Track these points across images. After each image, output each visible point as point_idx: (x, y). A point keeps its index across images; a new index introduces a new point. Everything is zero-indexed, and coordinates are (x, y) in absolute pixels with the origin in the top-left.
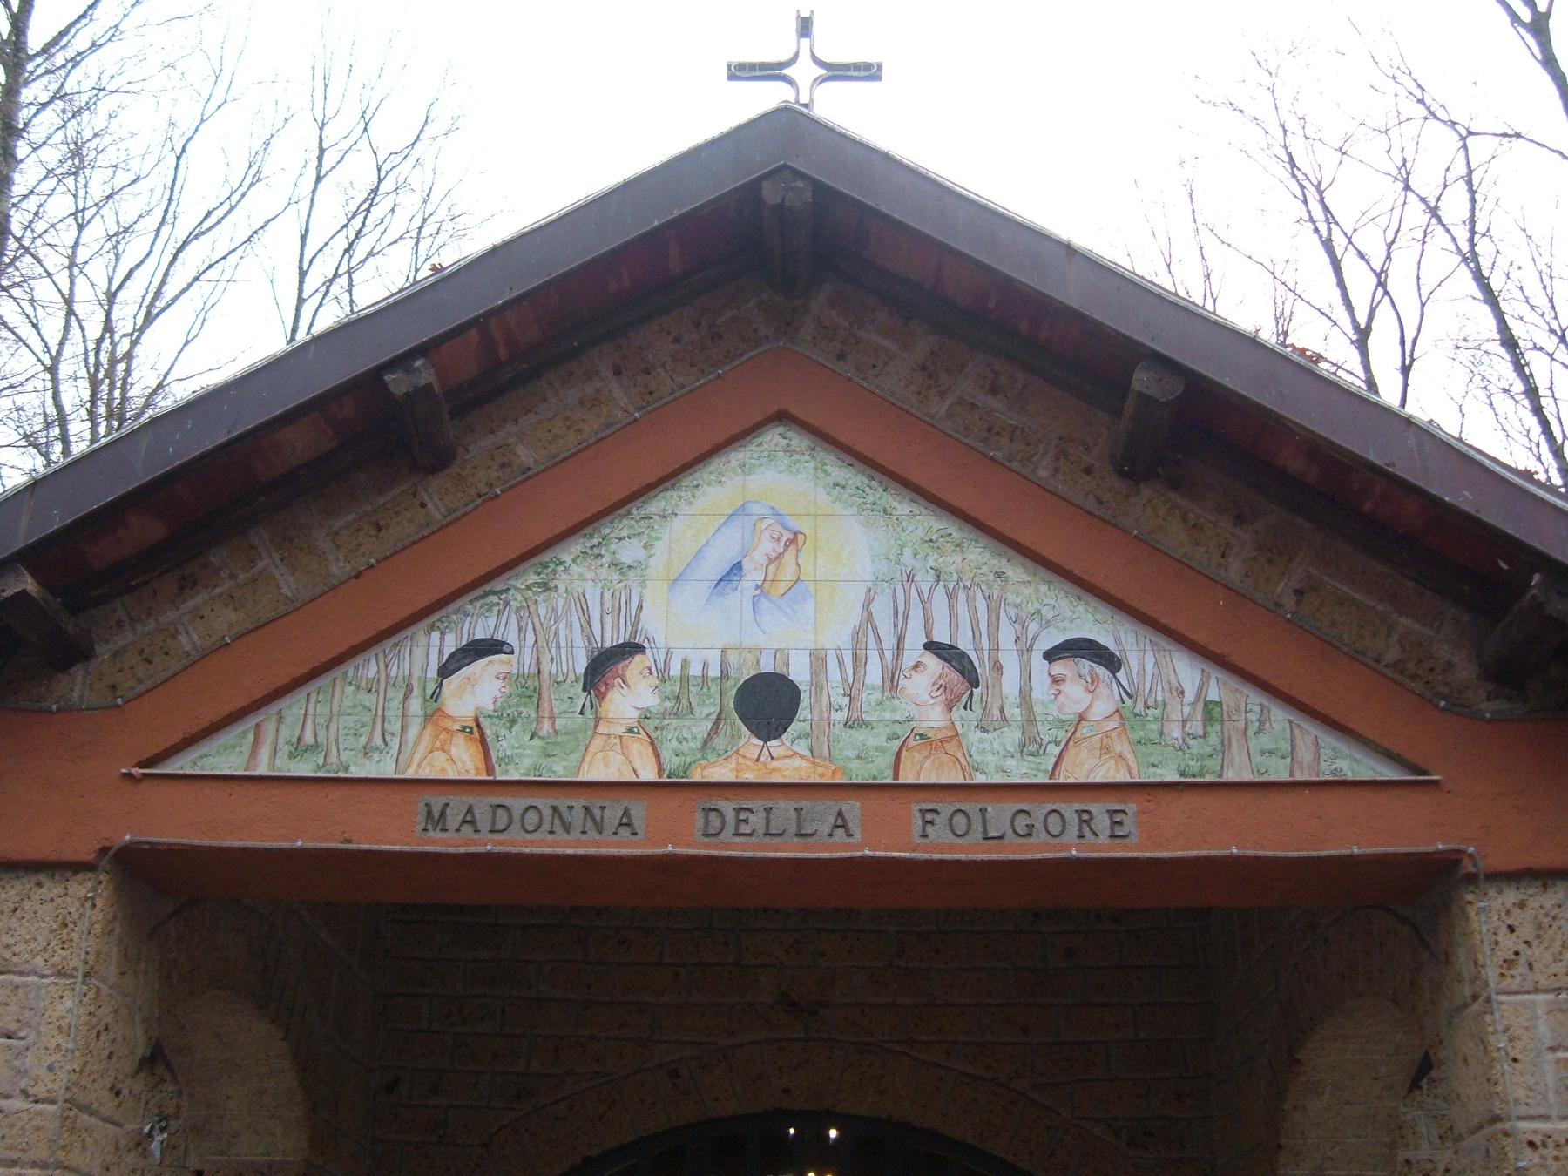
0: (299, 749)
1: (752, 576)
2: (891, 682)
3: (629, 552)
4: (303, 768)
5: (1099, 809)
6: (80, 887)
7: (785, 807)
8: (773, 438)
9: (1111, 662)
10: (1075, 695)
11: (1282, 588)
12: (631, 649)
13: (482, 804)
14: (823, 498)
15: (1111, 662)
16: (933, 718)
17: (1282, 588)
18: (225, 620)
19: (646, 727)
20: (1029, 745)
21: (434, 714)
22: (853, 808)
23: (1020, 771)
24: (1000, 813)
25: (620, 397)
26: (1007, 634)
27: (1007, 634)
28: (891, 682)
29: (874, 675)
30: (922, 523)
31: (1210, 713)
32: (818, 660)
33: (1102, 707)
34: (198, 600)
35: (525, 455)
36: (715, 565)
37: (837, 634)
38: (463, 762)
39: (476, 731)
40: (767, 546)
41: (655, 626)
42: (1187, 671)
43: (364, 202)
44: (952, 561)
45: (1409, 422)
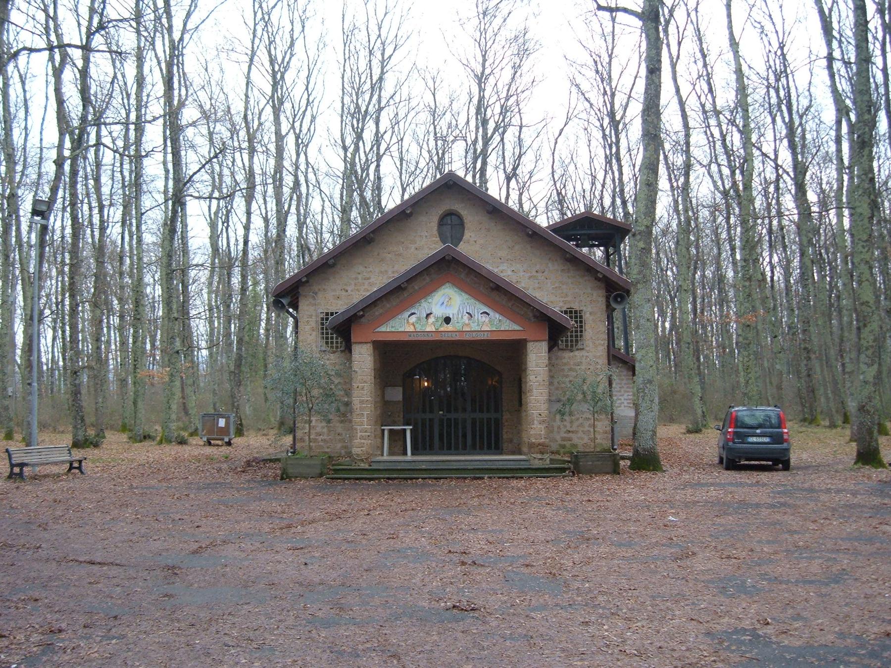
0: (392, 327)
1: (445, 304)
2: (462, 317)
3: (430, 301)
4: (393, 330)
5: (486, 333)
6: (369, 345)
7: (450, 333)
8: (447, 285)
9: (488, 314)
10: (484, 319)
11: (510, 305)
12: (431, 313)
13: (415, 334)
14: (453, 293)
15: (488, 314)
16: (467, 322)
17: (510, 305)
18: (381, 311)
19: (433, 323)
20: (478, 325)
21: (408, 322)
22: (457, 334)
23: (477, 328)
24: (474, 334)
25: (428, 279)
26: (476, 311)
27: (476, 311)
28: (462, 317)
29: (460, 316)
30: (465, 296)
31: (500, 321)
32: (453, 315)
33: (487, 320)
34: (376, 308)
35: (416, 288)
36: (440, 303)
37: (455, 312)
38: (411, 329)
39: (413, 324)
40: (447, 300)
41: (434, 311)
42: (497, 316)
43: (55, 12)
44: (470, 301)
45: (656, 194)
